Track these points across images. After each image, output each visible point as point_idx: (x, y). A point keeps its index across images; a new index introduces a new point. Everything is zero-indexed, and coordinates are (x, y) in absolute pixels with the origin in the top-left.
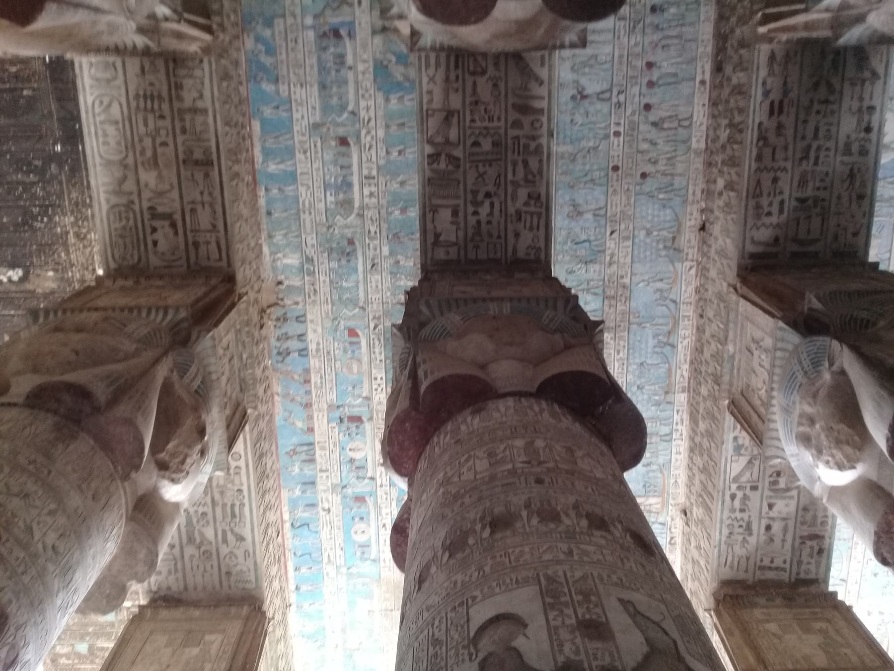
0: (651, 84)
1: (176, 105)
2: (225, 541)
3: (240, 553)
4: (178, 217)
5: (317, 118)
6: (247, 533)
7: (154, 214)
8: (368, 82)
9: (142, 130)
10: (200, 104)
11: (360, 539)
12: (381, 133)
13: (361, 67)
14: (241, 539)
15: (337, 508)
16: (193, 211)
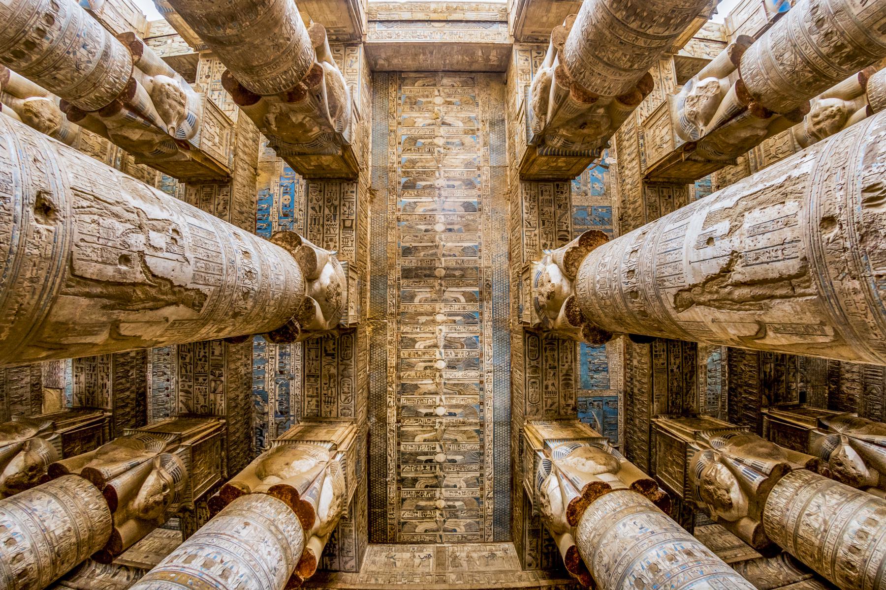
0: (167, 389)
1: (319, 399)
2: (320, 207)
3: (314, 201)
4: (324, 354)
5: (291, 382)
6: (310, 211)
7: (332, 355)
8: (271, 395)
9: (333, 390)
10: (310, 399)
11: (287, 197)
12: (267, 375)
13: (273, 401)
14: (313, 208)
15: (296, 211)
16: (317, 357)
